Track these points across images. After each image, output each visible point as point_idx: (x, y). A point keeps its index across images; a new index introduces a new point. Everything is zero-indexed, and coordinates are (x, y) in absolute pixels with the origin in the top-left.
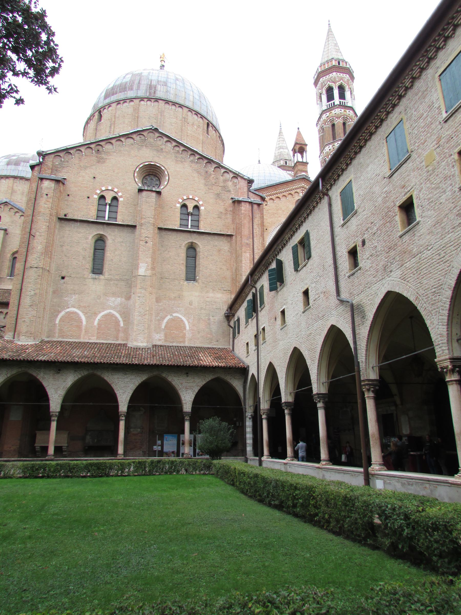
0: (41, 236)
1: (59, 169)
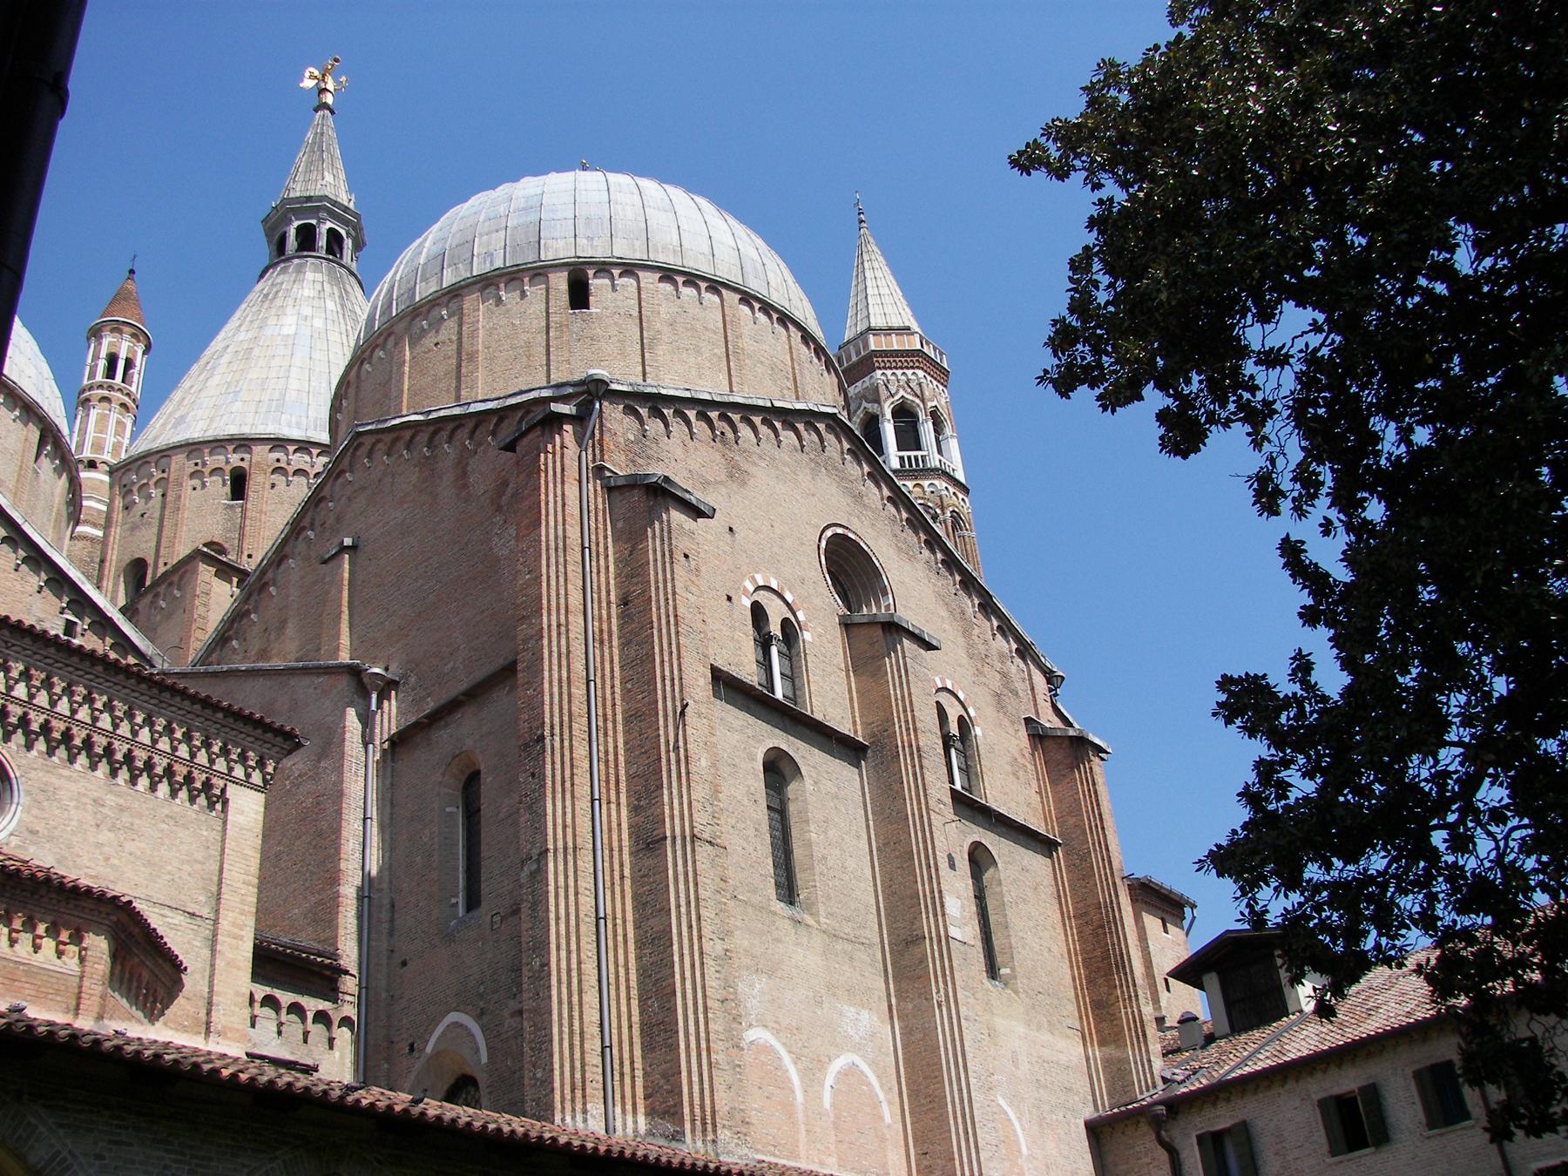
0: (699, 715)
1: (640, 461)
